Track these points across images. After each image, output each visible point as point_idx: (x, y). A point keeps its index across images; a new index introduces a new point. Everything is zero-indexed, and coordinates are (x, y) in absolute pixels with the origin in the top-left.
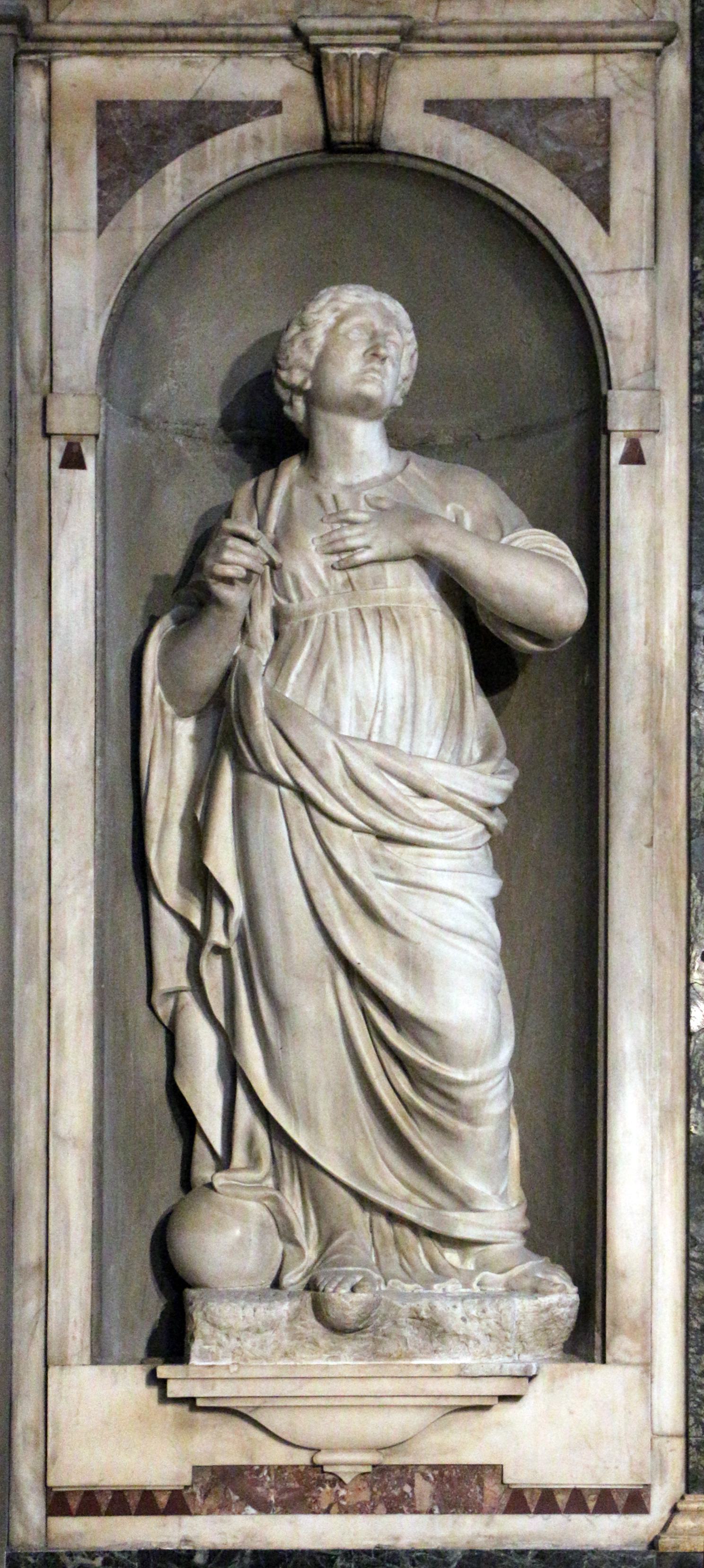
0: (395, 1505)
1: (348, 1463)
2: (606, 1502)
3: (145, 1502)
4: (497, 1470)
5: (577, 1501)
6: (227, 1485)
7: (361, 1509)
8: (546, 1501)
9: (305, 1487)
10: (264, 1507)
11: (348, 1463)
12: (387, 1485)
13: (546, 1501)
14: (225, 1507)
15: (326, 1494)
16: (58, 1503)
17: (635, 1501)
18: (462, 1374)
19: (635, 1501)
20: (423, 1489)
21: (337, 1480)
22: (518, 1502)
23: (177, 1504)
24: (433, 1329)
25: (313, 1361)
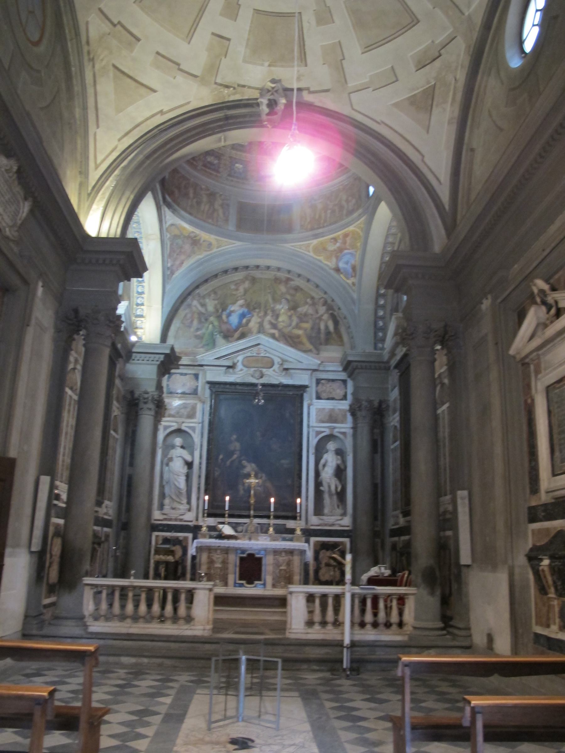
9: (170, 520)
12: (176, 520)
17: (191, 521)
19: (191, 521)
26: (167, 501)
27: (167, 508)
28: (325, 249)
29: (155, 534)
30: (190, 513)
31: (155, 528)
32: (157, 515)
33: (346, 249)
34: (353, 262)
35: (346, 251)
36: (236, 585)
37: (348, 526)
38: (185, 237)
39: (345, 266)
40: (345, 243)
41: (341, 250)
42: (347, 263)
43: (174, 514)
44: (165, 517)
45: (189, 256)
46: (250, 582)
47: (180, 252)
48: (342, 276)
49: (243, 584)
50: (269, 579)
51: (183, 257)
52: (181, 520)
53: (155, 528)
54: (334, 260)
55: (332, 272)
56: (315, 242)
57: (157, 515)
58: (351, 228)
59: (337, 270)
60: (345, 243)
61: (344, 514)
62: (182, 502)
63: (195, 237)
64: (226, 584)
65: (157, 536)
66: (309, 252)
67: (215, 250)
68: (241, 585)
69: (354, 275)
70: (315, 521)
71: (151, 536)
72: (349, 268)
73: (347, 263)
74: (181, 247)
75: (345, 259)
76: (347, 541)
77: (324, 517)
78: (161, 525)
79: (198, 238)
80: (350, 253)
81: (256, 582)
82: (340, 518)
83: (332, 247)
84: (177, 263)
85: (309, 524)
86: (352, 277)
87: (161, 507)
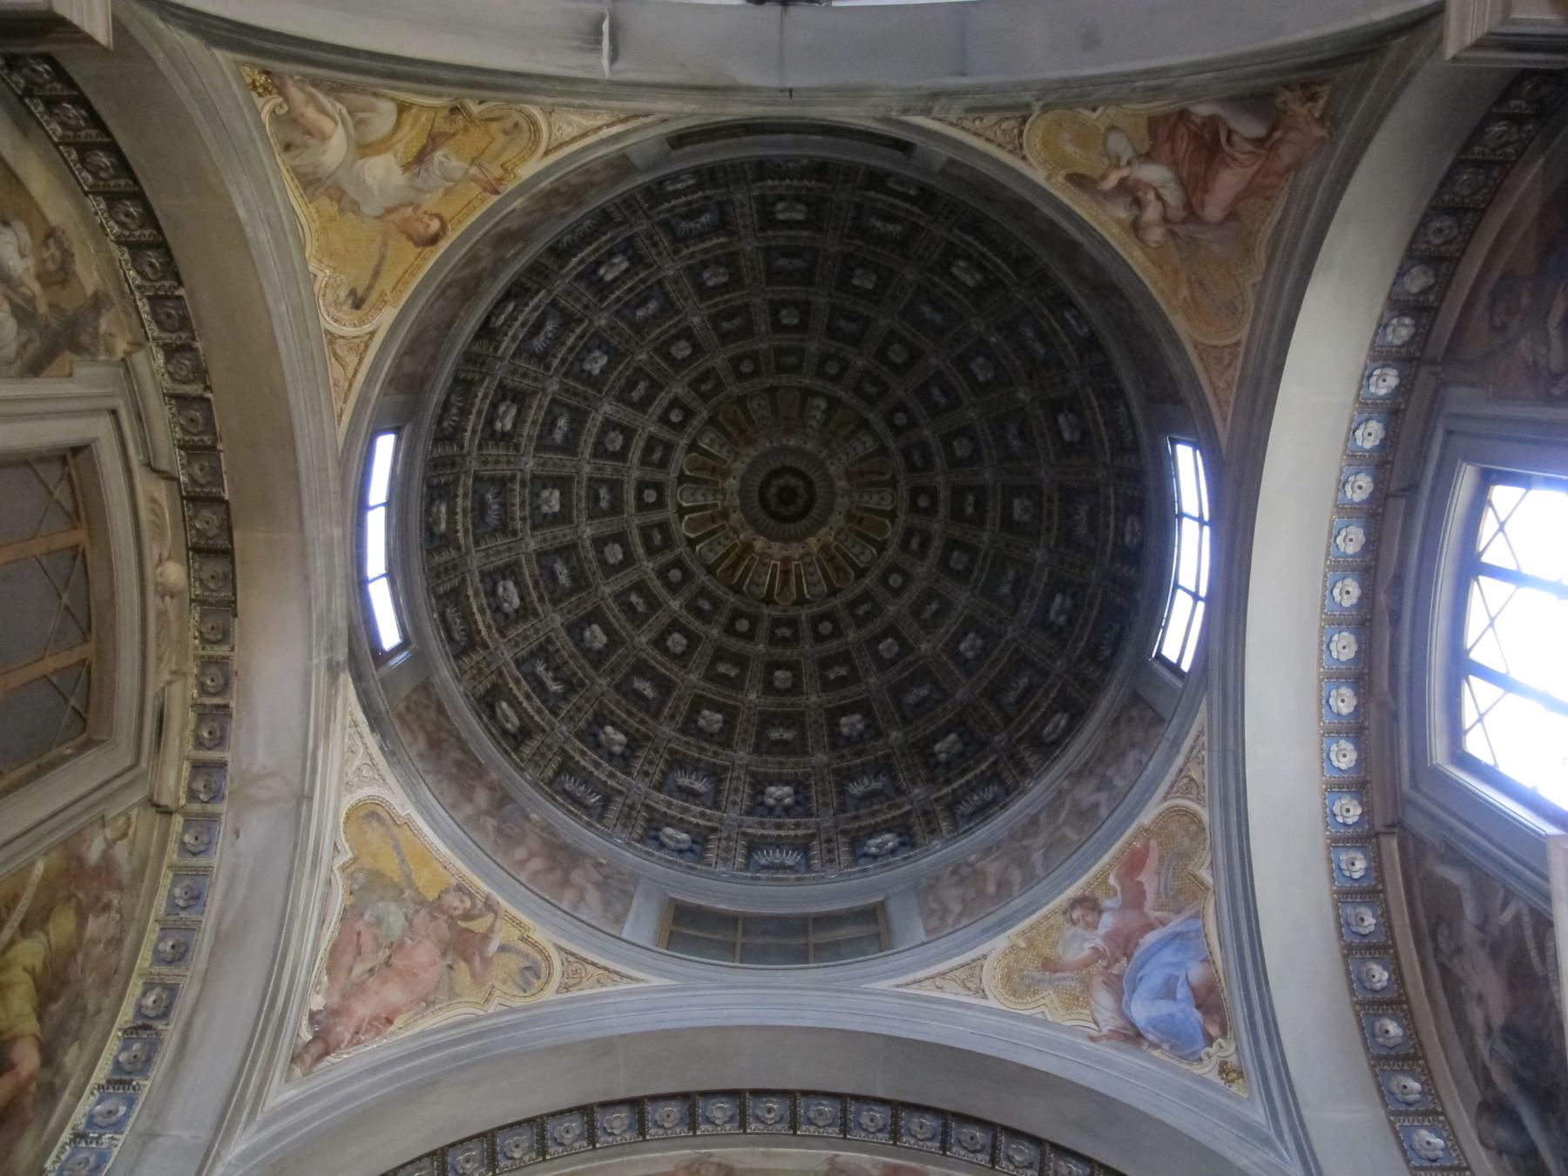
28: (1050, 965)
33: (1150, 927)
34: (1196, 973)
35: (1150, 938)
38: (422, 903)
39: (1164, 1008)
40: (1135, 899)
41: (1124, 943)
42: (1168, 992)
45: (428, 1003)
47: (387, 964)
48: (1156, 1053)
51: (393, 994)
54: (1104, 999)
55: (1104, 1049)
56: (1001, 943)
58: (1147, 817)
59: (1132, 1036)
60: (1135, 899)
63: (468, 916)
66: (985, 997)
67: (549, 995)
69: (1214, 1030)
72: (1184, 1010)
73: (1168, 992)
74: (397, 947)
75: (1155, 976)
79: (479, 926)
80: (1175, 936)
83: (1079, 945)
84: (363, 1009)
86: (1210, 1040)
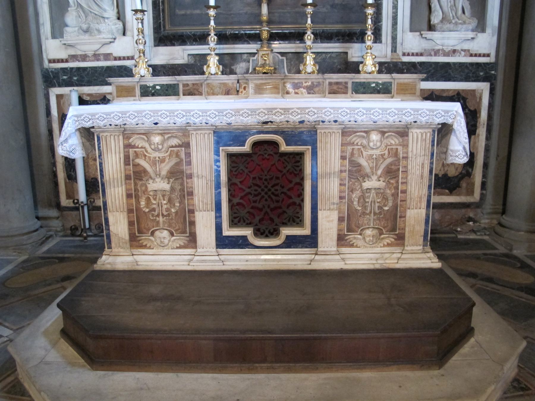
0: (98, 60)
1: (90, 53)
2: (128, 58)
3: (62, 61)
4: (112, 54)
5: (124, 58)
6: (74, 58)
7: (93, 61)
8: (120, 59)
9: (84, 58)
10: (79, 61)
11: (90, 53)
12: (96, 57)
13: (120, 59)
14: (73, 61)
15: (88, 59)
16: (50, 61)
18: (104, 38)
20: (102, 57)
21: (89, 57)
22: (115, 59)
23: (67, 61)
24: (99, 31)
25: (82, 37)
26: (71, 18)
27: (71, 33)
29: (54, 92)
30: (127, 39)
31: (53, 79)
32: (53, 50)
36: (223, 242)
37: (488, 55)
43: (88, 45)
44: (72, 52)
46: (267, 230)
49: (244, 238)
50: (329, 224)
52: (107, 57)
53: (53, 79)
57: (53, 50)
61: (481, 27)
62: (106, 15)
64: (192, 241)
65: (59, 97)
68: (240, 243)
70: (412, 44)
71: (47, 97)
76: (483, 87)
77: (435, 35)
78: (64, 70)
81: (286, 231)
82: (471, 35)
85: (399, 51)
87: (58, 31)
